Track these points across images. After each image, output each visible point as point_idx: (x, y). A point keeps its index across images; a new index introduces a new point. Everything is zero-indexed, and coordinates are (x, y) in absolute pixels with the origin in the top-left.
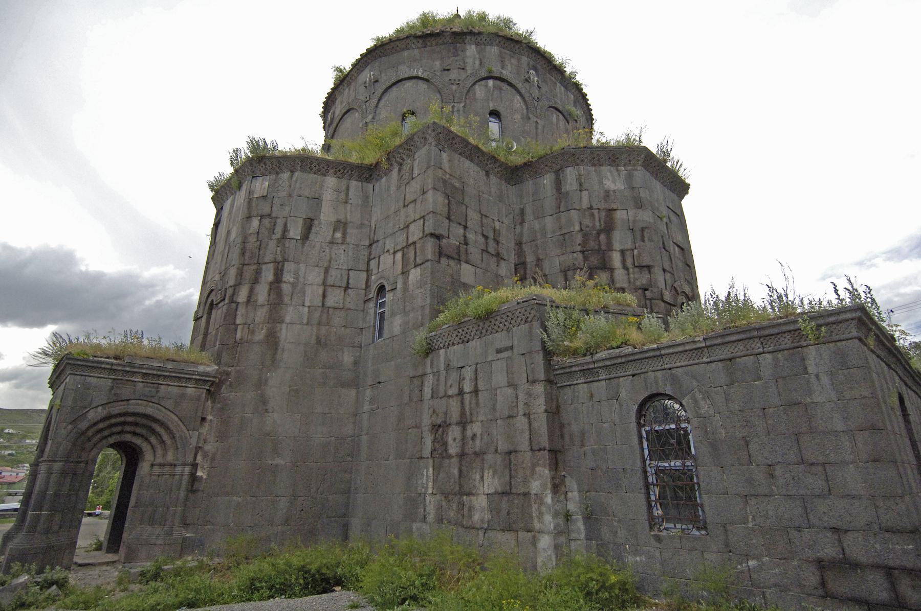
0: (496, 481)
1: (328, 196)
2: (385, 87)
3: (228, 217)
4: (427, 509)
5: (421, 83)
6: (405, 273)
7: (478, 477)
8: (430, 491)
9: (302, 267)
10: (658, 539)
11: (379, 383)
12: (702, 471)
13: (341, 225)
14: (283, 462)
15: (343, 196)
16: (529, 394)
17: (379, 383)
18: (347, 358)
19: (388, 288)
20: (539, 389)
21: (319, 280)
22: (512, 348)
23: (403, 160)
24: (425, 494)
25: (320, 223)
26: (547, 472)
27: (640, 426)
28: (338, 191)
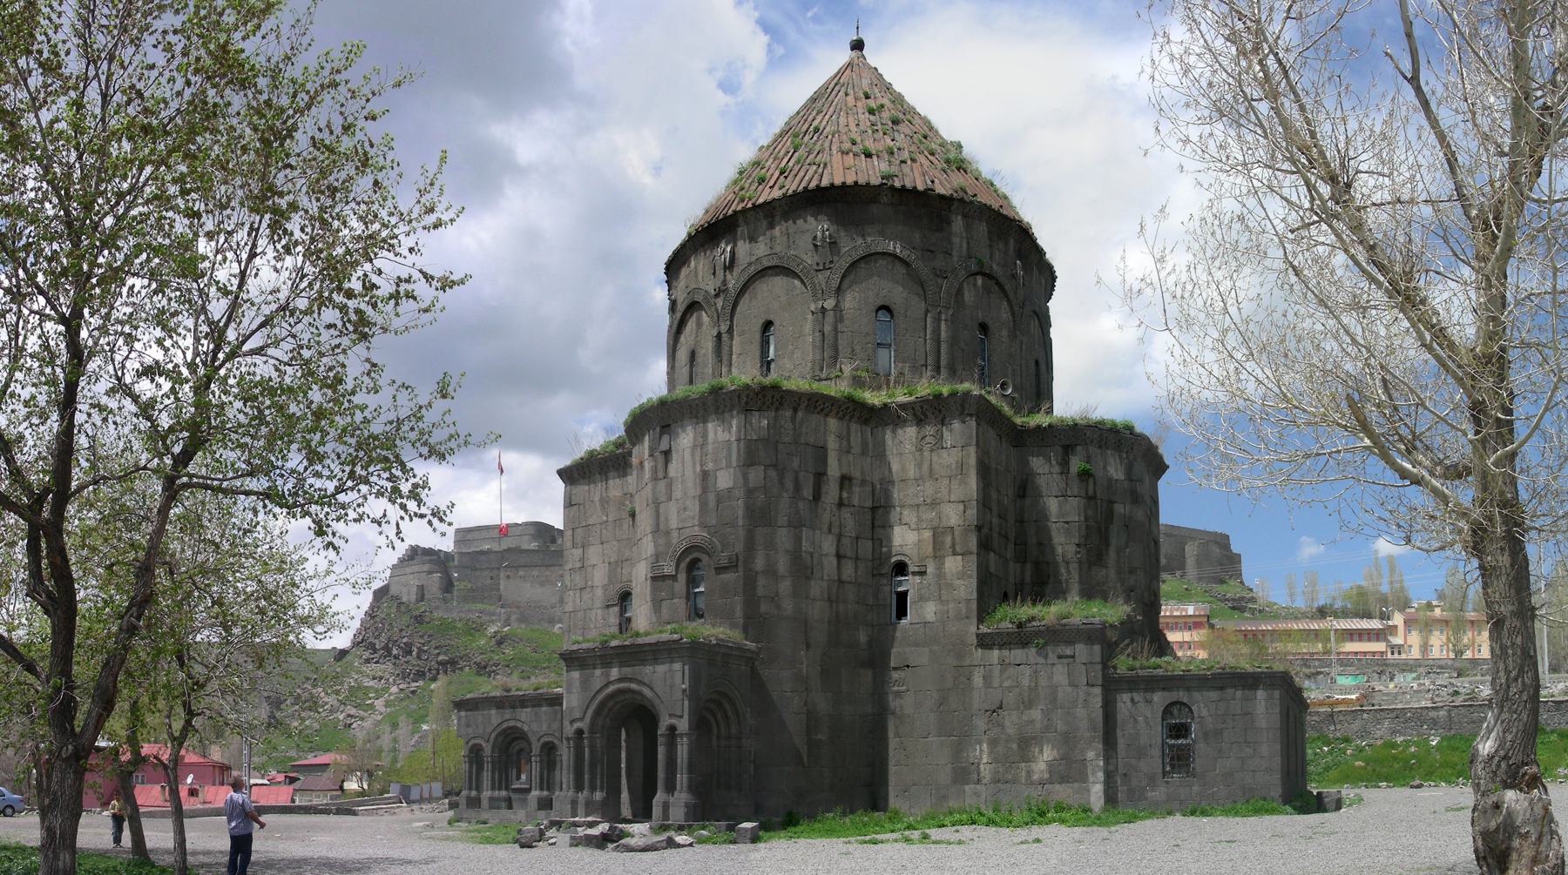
0: (1055, 751)
1: (832, 444)
2: (850, 260)
3: (695, 446)
4: (982, 775)
5: (898, 264)
6: (938, 556)
7: (1037, 750)
8: (985, 761)
9: (817, 531)
10: (1167, 783)
11: (908, 666)
12: (1197, 746)
13: (845, 480)
14: (824, 738)
15: (845, 443)
16: (1088, 694)
17: (908, 666)
18: (863, 637)
19: (912, 568)
20: (1098, 691)
21: (833, 550)
22: (1073, 657)
23: (926, 416)
24: (979, 764)
25: (828, 479)
26: (1101, 746)
27: (1163, 719)
28: (839, 437)
